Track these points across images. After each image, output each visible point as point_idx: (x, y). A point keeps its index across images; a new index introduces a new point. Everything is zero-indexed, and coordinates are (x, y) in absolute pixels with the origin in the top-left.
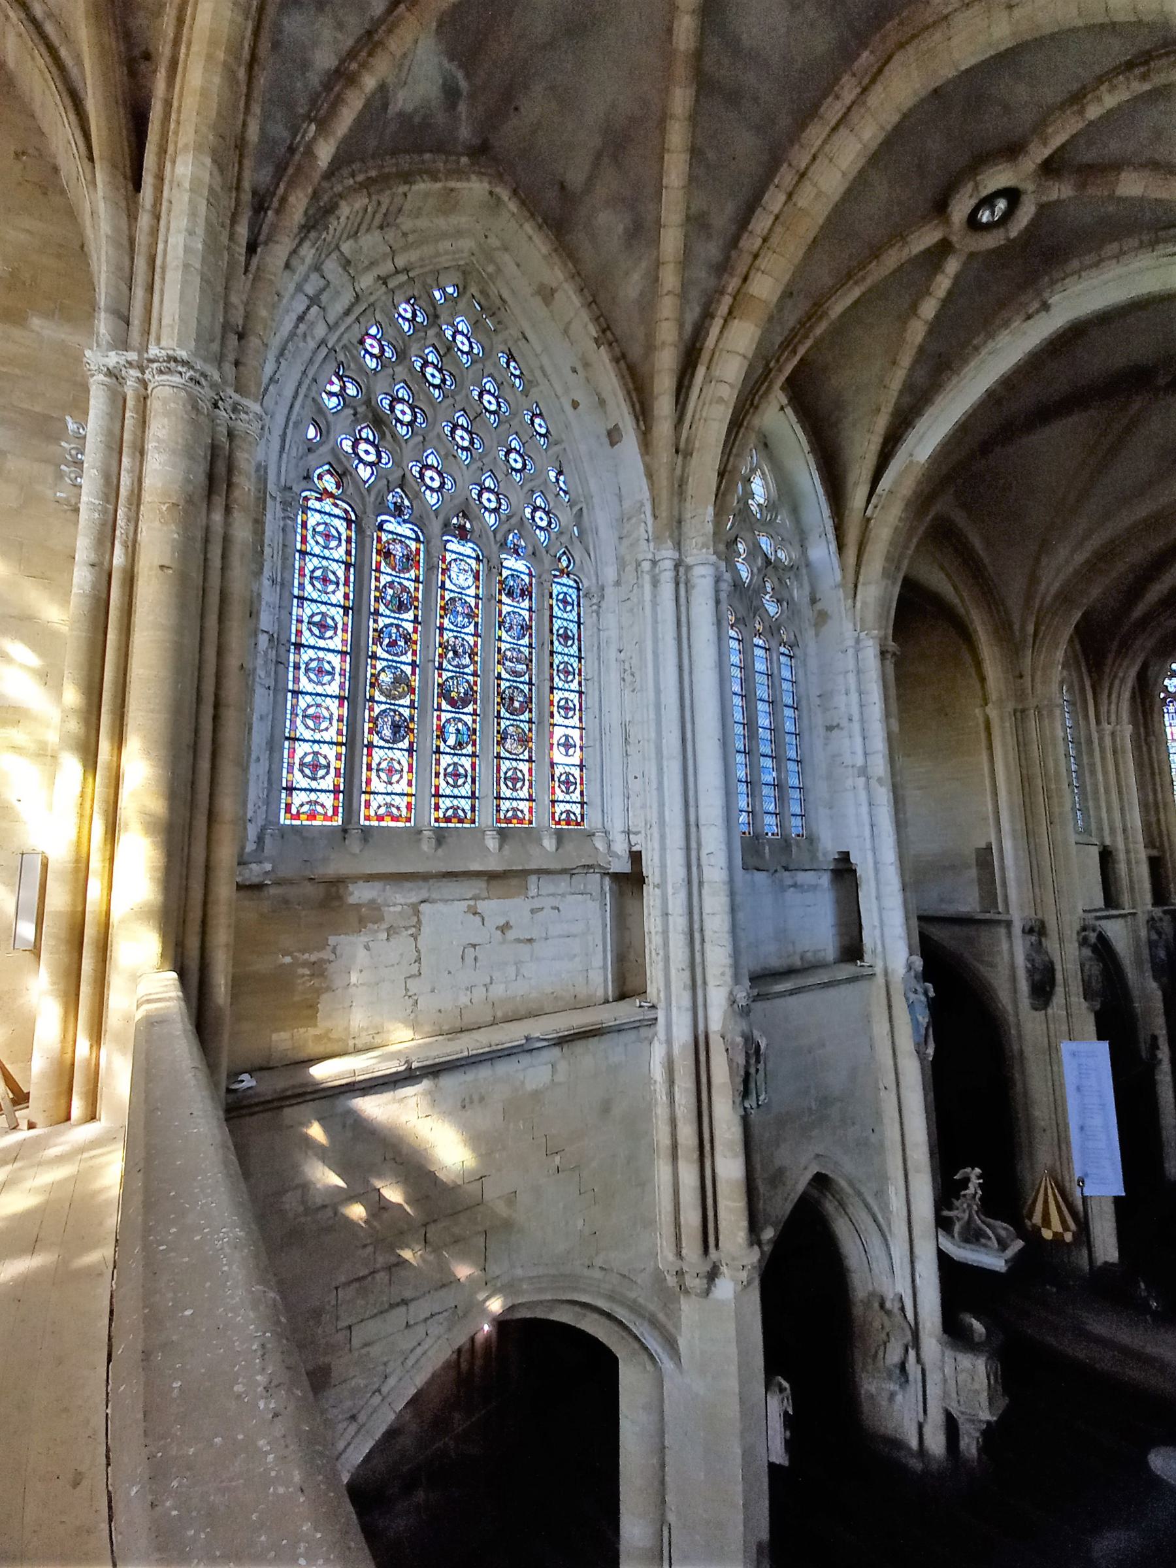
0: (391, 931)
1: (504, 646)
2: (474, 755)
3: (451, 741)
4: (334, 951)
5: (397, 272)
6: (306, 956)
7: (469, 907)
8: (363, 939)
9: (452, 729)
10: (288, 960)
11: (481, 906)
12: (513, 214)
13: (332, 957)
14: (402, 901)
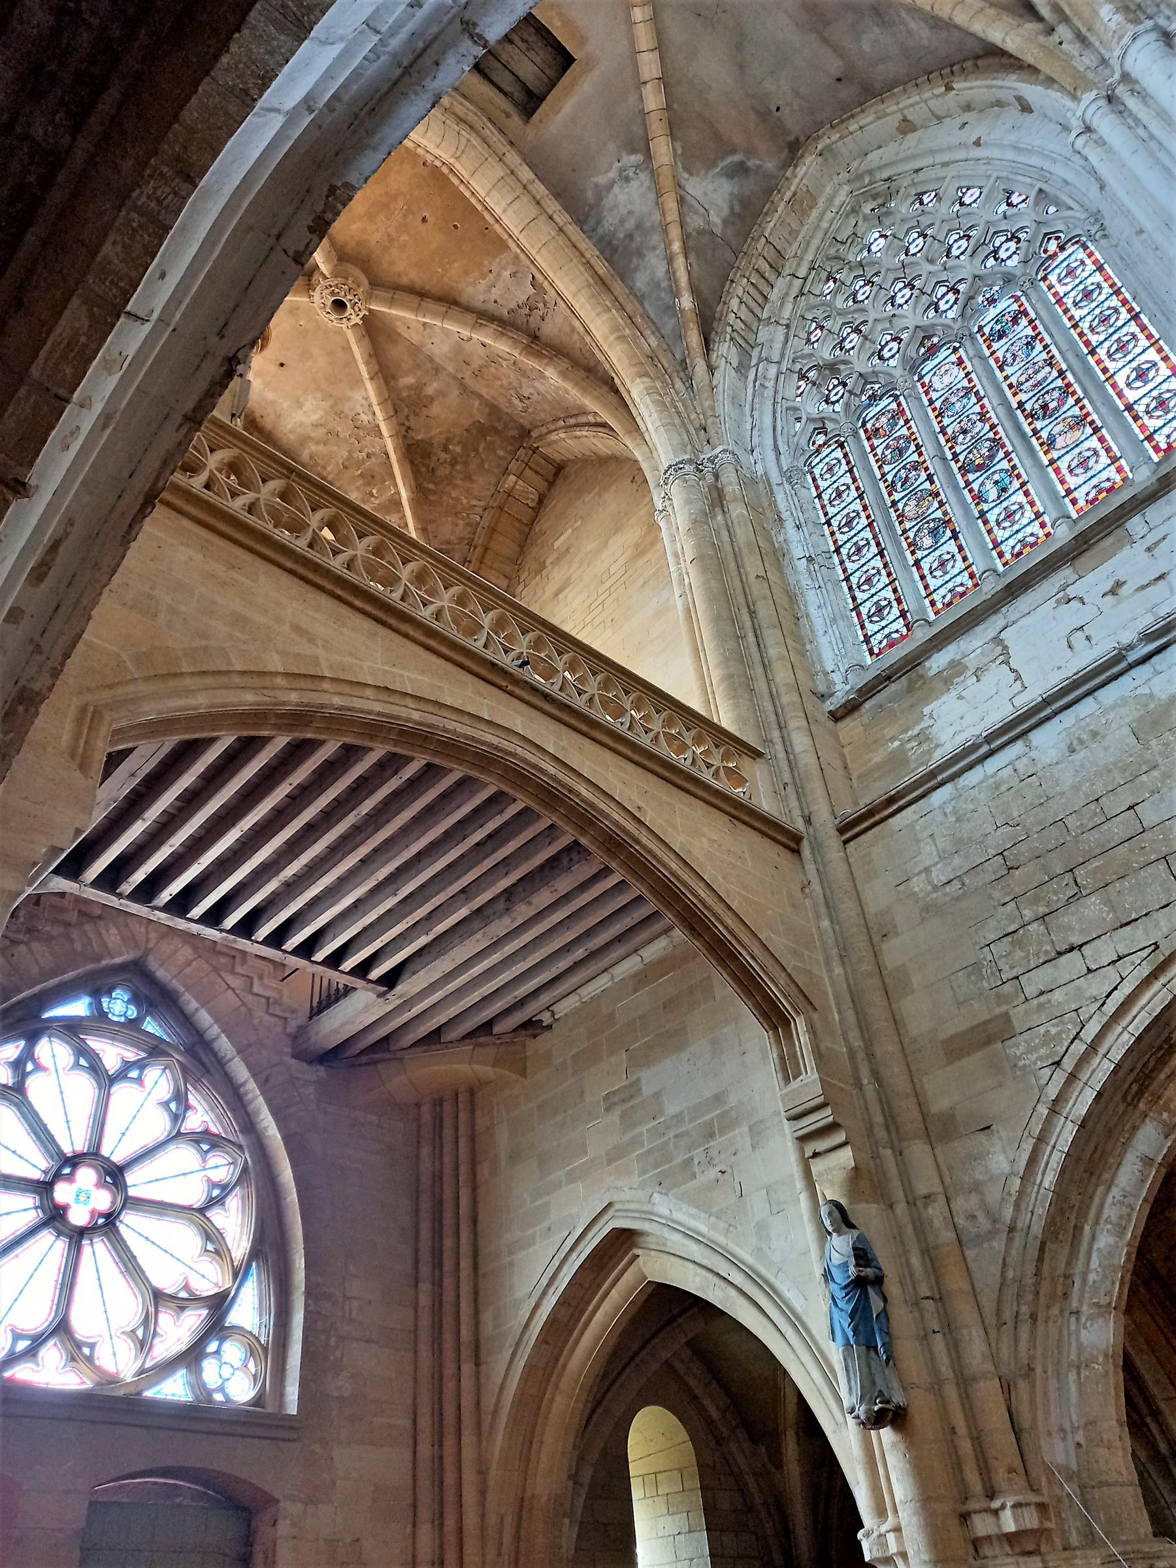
0: (978, 674)
1: (1013, 380)
2: (1023, 485)
3: (993, 494)
4: (931, 716)
5: (805, 279)
6: (910, 733)
7: (1058, 602)
8: (953, 693)
9: (989, 485)
10: (896, 743)
11: (1071, 592)
12: (841, 138)
13: (931, 722)
14: (980, 643)
